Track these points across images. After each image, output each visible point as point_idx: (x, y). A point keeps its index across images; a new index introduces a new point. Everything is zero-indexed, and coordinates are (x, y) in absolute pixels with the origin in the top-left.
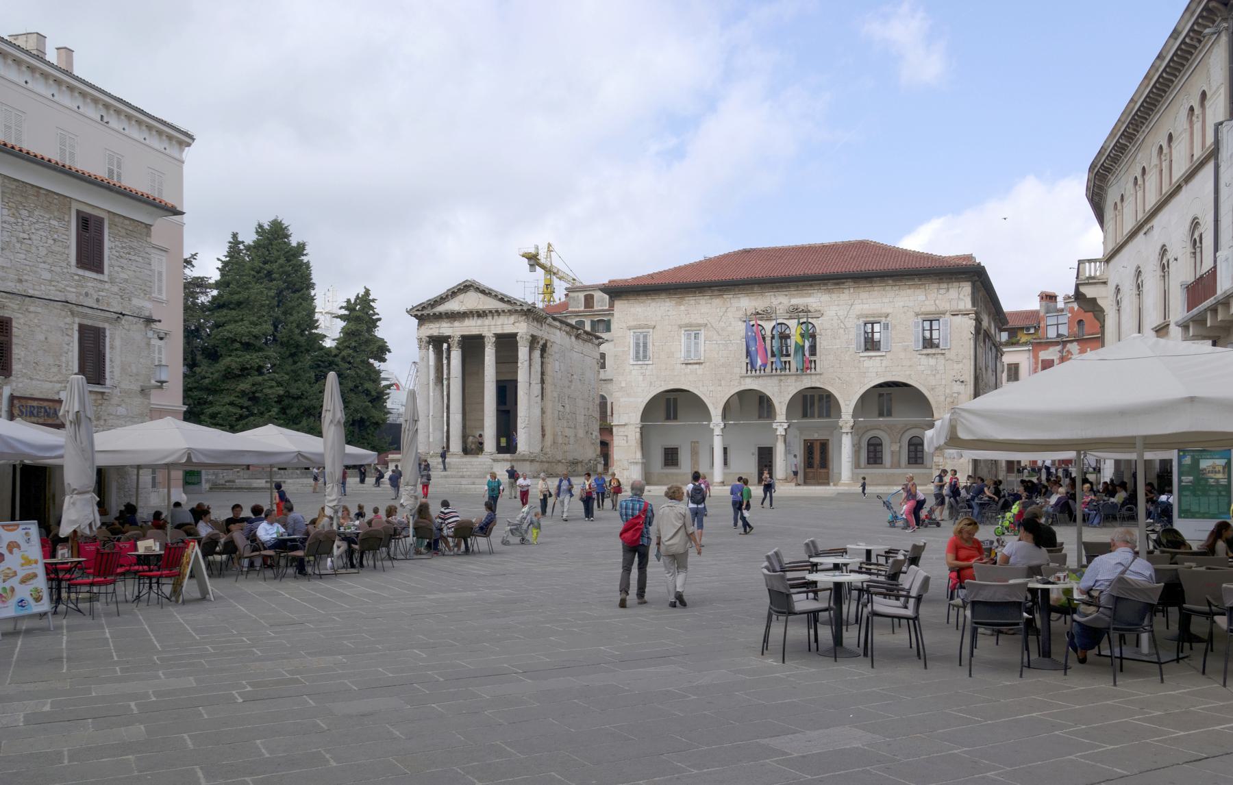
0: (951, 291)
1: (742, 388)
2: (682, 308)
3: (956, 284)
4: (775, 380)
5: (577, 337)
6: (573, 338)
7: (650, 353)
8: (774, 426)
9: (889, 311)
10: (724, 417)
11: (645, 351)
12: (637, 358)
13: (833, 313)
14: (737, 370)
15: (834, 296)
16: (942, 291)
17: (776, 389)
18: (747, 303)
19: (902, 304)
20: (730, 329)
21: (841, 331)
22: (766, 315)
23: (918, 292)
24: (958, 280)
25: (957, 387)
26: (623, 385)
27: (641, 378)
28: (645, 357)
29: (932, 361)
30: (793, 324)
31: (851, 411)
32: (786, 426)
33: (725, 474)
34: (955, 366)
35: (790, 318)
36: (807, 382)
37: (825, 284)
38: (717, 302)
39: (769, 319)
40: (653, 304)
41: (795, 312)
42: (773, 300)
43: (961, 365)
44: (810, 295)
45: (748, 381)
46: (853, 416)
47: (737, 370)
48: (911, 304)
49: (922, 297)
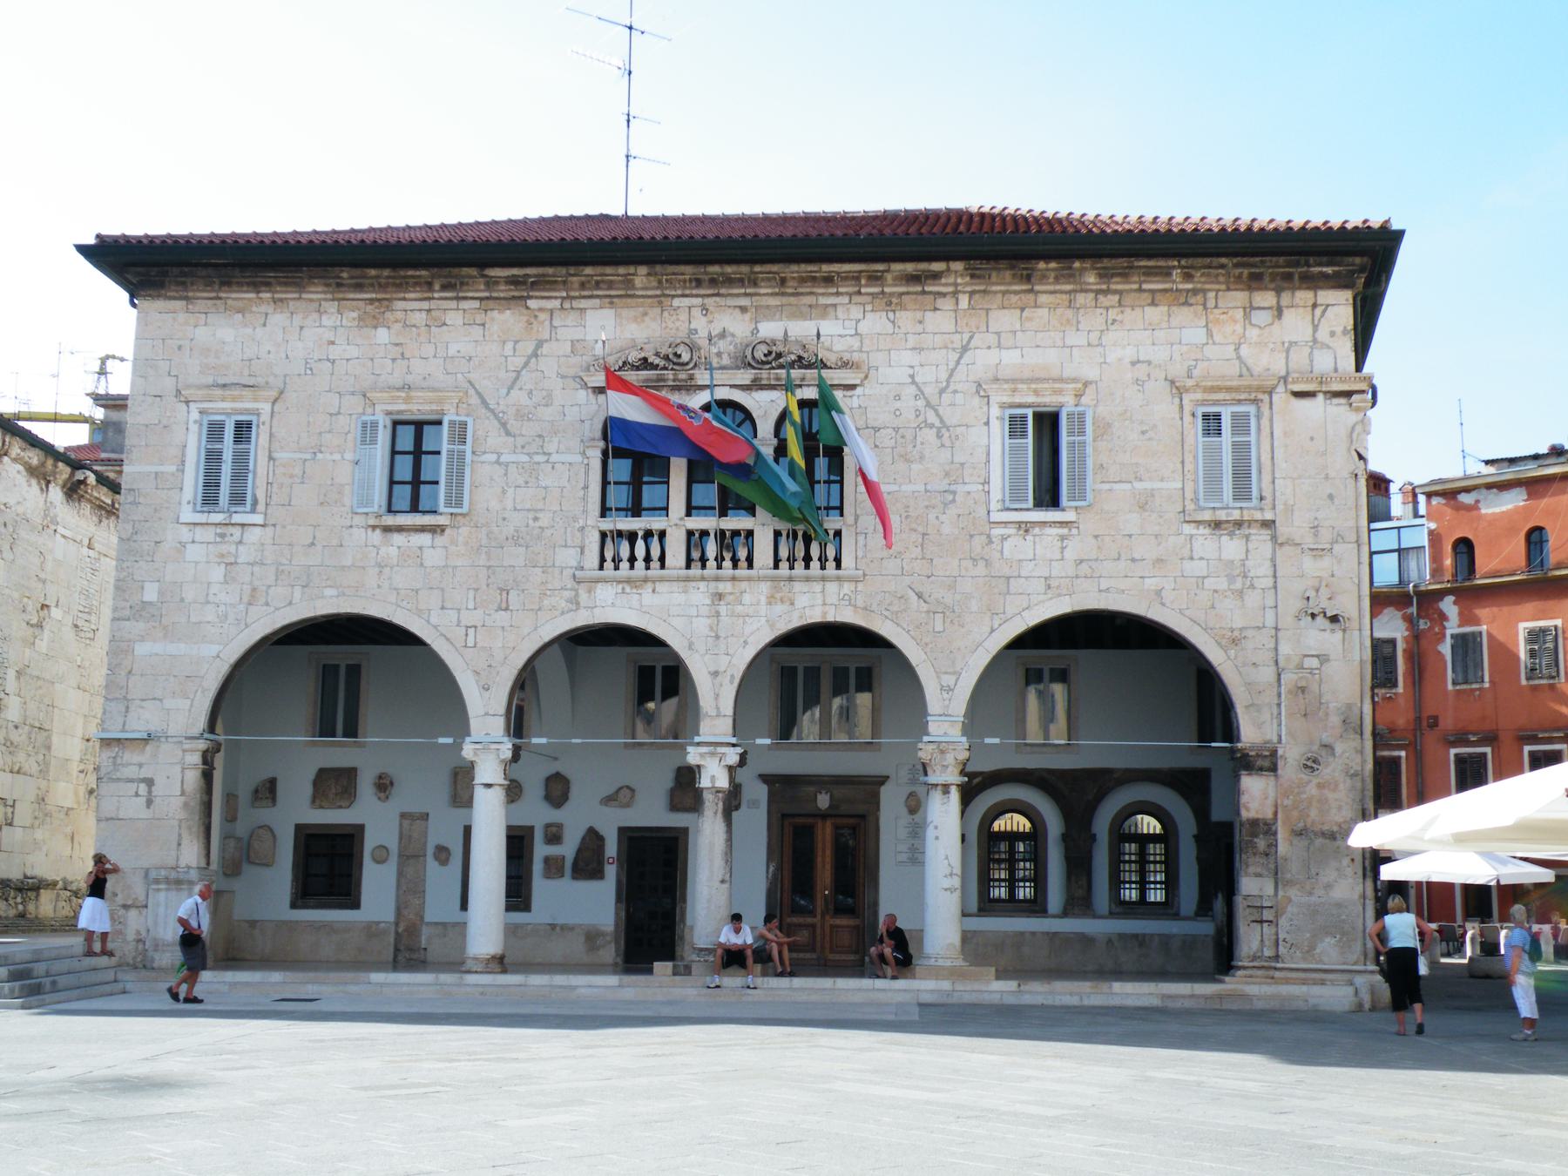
0: (1288, 315)
1: (582, 619)
2: (382, 335)
3: (1304, 296)
4: (699, 595)
5: (73, 490)
6: (56, 493)
7: (257, 484)
9: (1091, 373)
10: (517, 723)
11: (240, 475)
12: (209, 498)
13: (901, 375)
14: (568, 557)
15: (906, 318)
16: (1260, 317)
17: (702, 625)
18: (606, 326)
19: (1129, 353)
20: (547, 413)
21: (930, 435)
23: (1183, 314)
24: (1313, 282)
25: (1319, 638)
26: (151, 594)
27: (218, 573)
28: (238, 498)
29: (1232, 547)
30: (765, 405)
31: (959, 704)
32: (732, 757)
33: (511, 931)
34: (1310, 565)
35: (756, 385)
36: (817, 601)
37: (875, 278)
38: (506, 320)
40: (278, 319)
41: (770, 362)
42: (700, 324)
43: (1326, 562)
44: (824, 312)
45: (605, 593)
48: (1159, 354)
49: (1196, 334)
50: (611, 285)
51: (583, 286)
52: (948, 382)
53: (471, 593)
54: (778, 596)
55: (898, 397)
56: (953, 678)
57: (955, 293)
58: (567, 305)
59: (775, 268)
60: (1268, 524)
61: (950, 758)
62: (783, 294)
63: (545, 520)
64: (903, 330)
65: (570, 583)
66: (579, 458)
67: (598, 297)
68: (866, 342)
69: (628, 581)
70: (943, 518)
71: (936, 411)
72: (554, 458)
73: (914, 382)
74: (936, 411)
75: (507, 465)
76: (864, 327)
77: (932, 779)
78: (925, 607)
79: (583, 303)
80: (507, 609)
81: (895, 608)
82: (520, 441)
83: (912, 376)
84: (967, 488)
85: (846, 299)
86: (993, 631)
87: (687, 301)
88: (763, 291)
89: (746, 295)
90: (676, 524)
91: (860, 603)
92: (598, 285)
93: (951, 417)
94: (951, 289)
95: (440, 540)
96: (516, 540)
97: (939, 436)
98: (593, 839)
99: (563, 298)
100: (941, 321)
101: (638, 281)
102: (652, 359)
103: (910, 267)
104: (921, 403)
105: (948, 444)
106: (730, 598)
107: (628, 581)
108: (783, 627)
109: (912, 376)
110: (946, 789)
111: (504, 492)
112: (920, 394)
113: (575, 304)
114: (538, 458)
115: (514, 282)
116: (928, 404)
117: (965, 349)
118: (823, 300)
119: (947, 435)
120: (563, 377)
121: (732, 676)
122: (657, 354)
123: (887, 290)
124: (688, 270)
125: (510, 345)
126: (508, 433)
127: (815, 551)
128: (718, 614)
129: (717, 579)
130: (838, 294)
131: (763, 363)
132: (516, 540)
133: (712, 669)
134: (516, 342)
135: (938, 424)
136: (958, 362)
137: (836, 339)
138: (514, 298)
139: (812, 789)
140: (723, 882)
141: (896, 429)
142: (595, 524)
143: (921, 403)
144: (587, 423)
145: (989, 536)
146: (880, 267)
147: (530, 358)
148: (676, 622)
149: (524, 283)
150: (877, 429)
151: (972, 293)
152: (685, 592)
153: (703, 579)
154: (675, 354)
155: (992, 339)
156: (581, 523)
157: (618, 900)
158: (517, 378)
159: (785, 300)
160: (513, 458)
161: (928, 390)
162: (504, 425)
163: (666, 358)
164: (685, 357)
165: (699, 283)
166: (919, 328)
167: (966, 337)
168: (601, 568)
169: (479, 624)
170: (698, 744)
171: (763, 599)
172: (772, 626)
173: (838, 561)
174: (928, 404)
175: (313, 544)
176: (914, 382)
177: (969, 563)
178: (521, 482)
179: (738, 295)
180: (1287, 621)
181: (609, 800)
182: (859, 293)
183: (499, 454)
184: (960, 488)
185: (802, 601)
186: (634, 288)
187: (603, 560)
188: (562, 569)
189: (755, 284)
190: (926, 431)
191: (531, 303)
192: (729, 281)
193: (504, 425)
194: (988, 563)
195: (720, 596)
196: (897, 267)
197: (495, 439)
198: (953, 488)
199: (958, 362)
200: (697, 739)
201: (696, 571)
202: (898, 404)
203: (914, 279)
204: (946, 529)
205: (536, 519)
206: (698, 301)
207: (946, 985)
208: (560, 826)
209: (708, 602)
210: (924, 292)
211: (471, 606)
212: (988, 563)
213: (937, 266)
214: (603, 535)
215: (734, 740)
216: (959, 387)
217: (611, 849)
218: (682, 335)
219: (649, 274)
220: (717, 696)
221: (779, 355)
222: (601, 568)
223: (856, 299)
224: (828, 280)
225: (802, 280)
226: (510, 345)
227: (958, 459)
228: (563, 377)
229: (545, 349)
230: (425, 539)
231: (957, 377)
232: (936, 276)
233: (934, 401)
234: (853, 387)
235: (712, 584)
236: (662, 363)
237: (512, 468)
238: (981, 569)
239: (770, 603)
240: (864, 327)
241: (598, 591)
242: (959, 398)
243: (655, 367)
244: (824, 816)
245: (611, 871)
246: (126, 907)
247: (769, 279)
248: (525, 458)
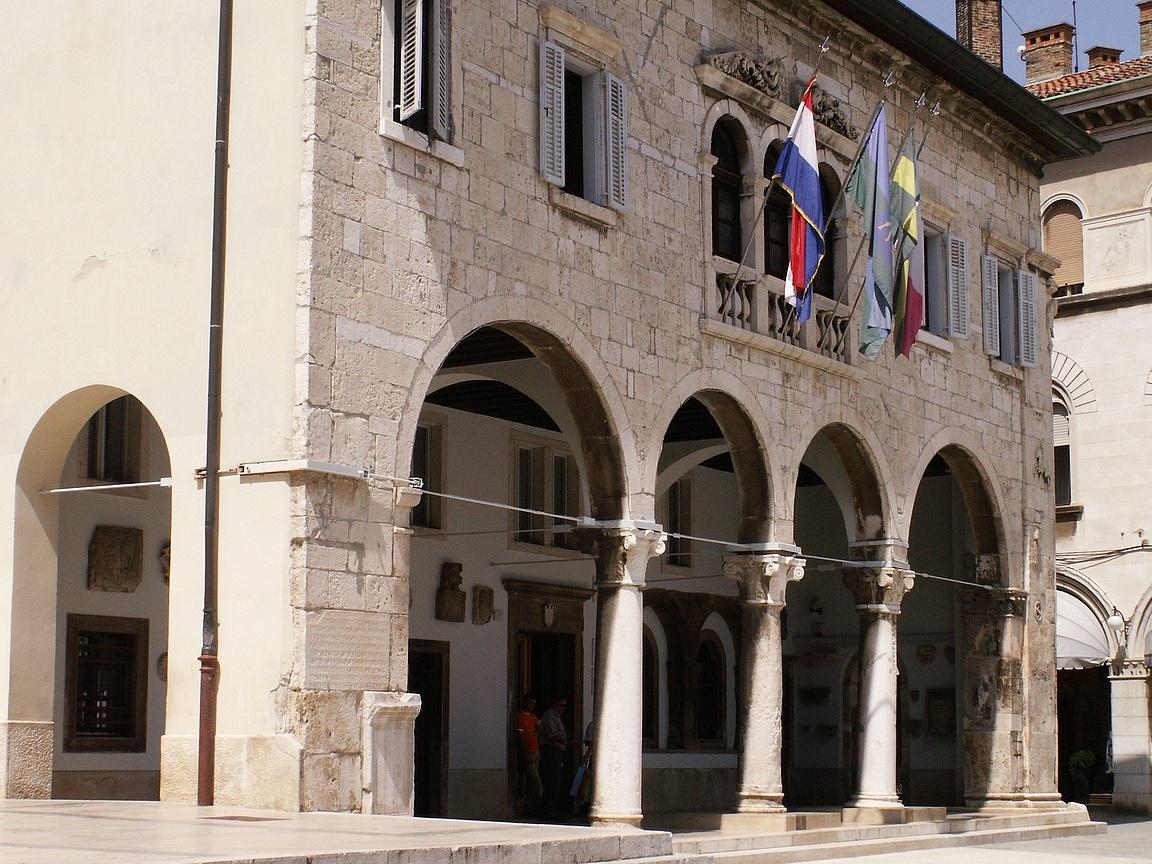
44: (827, 67)
47: (692, 296)
53: (629, 324)
60: (1019, 383)
75: (646, 159)
80: (655, 354)
95: (606, 245)
103: (882, 47)
126: (647, 120)
148: (762, 399)
162: (642, 103)
169: (636, 369)
175: (503, 213)
179: (785, 20)
180: (1030, 478)
185: (832, 395)
188: (692, 311)
193: (642, 103)
197: (638, 124)
206: (761, 13)
211: (630, 343)
213: (897, 56)
230: (591, 237)
246: (341, 754)
248: (658, 156)
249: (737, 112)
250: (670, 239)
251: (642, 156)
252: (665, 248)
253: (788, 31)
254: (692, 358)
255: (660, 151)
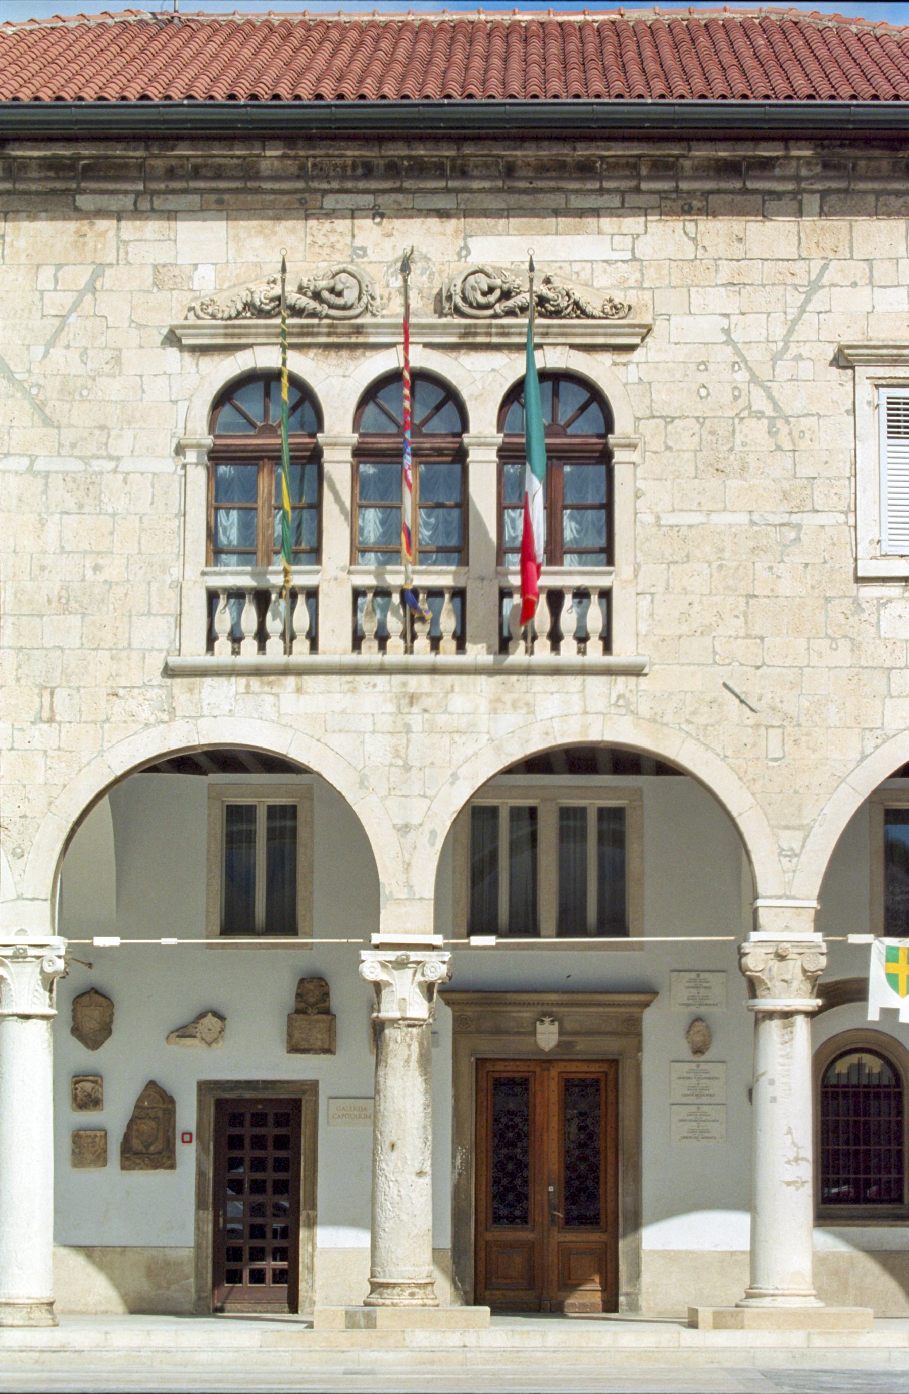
8: (371, 966)
13: (707, 327)
20: (113, 389)
21: (755, 430)
22: (325, 316)
30: (482, 379)
35: (467, 344)
37: (664, 168)
39: (350, 341)
46: (821, 923)
50: (219, 174)
51: (171, 173)
52: (786, 343)
54: (508, 698)
55: (703, 365)
56: (800, 835)
57: (795, 194)
58: (144, 205)
59: (499, 150)
61: (793, 969)
62: (511, 191)
63: (113, 570)
64: (711, 252)
65: (157, 679)
66: (168, 465)
67: (196, 191)
68: (651, 273)
69: (258, 672)
70: (780, 569)
71: (767, 390)
72: (125, 466)
73: (729, 342)
74: (767, 390)
75: (47, 475)
76: (645, 248)
77: (765, 1003)
78: (753, 718)
79: (173, 202)
80: (51, 720)
81: (702, 720)
82: (68, 436)
83: (727, 332)
84: (821, 519)
85: (615, 201)
86: (864, 757)
87: (348, 201)
88: (475, 185)
89: (448, 191)
90: (336, 573)
91: (644, 710)
92: (196, 173)
93: (794, 400)
94: (790, 186)
96: (64, 603)
97: (772, 432)
98: (156, 1103)
99: (138, 194)
100: (773, 236)
101: (264, 165)
102: (293, 297)
103: (723, 152)
104: (742, 376)
105: (787, 445)
106: (427, 702)
107: (258, 672)
108: (518, 752)
109: (727, 332)
110: (787, 1015)
111: (43, 523)
112: (740, 361)
113: (158, 203)
114: (96, 465)
115: (54, 166)
116: (754, 379)
117: (814, 286)
118: (576, 202)
119: (784, 429)
120: (140, 326)
121: (433, 833)
122: (301, 290)
123: (684, 186)
124: (352, 152)
125: (47, 273)
126: (48, 422)
127: (568, 620)
128: (408, 729)
129: (407, 670)
130: (601, 191)
131: (480, 307)
132: (64, 603)
133: (399, 822)
134: (59, 266)
135: (769, 412)
136: (803, 310)
137: (599, 267)
138: (53, 192)
139: (527, 1014)
140: (420, 1174)
141: (701, 420)
142: (195, 576)
143: (742, 376)
144: (182, 407)
145: (856, 600)
146: (675, 150)
147: (81, 294)
149: (72, 167)
150: (669, 420)
151: (824, 194)
152: (354, 691)
153: (382, 670)
154: (332, 291)
155: (858, 270)
156: (176, 572)
157: (200, 1204)
158: (60, 329)
159: (513, 200)
160: (56, 465)
161: (755, 355)
163: (317, 296)
164: (350, 296)
165: (368, 170)
166: (738, 250)
167: (816, 265)
168: (210, 647)
170: (377, 947)
171: (484, 706)
172: (498, 749)
173: (607, 639)
174: (754, 379)
176: (729, 342)
177: (822, 644)
178: (71, 505)
179: (434, 192)
181: (183, 1032)
182: (637, 190)
183: (33, 459)
184: (810, 520)
186: (256, 176)
187: (211, 638)
189: (463, 173)
190: (752, 423)
191: (81, 200)
192: (420, 169)
193: (40, 407)
194: (855, 646)
195: (412, 699)
196: (702, 152)
198: (795, 518)
199: (803, 310)
200: (376, 939)
201: (370, 654)
202: (703, 378)
203: (730, 168)
204: (786, 587)
205: (97, 568)
207: (797, 1338)
208: (96, 1078)
209: (391, 708)
210: (746, 191)
212: (855, 646)
213: (766, 151)
214: (212, 597)
215: (438, 940)
216: (805, 351)
217: (187, 1116)
218: (340, 260)
219: (284, 156)
220: (408, 866)
221: (506, 295)
222: (210, 647)
223: (633, 200)
224: (585, 169)
225: (542, 169)
226: (47, 273)
227: (805, 471)
228: (140, 326)
229: (108, 279)
231: (804, 331)
232: (766, 164)
233: (764, 372)
234: (631, 348)
235: (398, 679)
236: (313, 304)
237: (56, 481)
238: (843, 656)
239: (495, 711)
240: (645, 248)
241: (206, 691)
242: (805, 369)
243: (296, 311)
244: (547, 1061)
245: (188, 1156)
247: (487, 166)
248: (79, 466)
249: (266, 358)
250: (97, 568)
251: (36, 474)
252: (83, 580)
253: (442, 202)
254: (145, 714)
255: (81, 458)
